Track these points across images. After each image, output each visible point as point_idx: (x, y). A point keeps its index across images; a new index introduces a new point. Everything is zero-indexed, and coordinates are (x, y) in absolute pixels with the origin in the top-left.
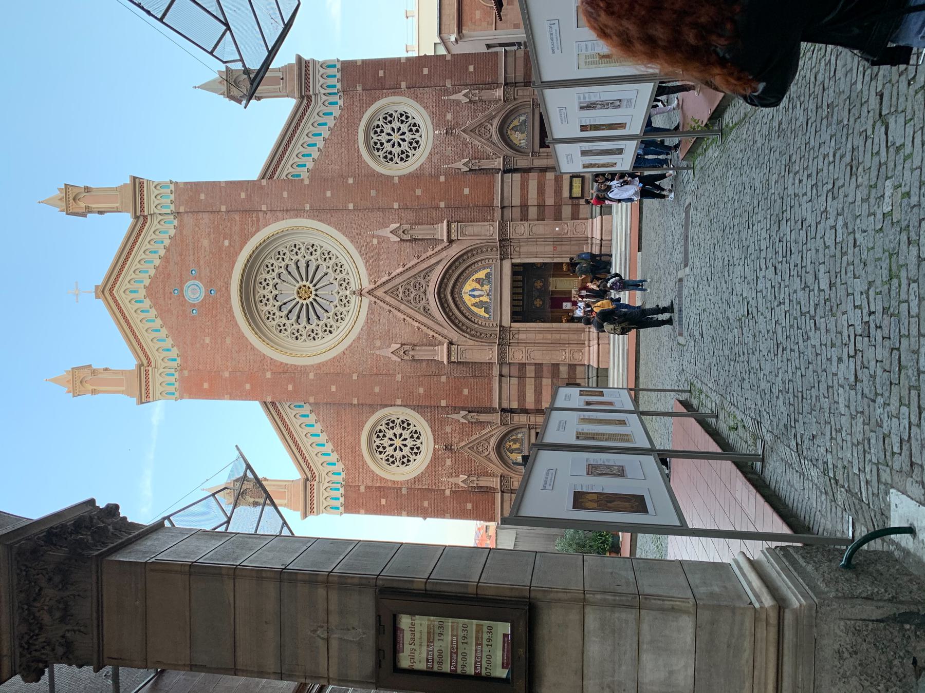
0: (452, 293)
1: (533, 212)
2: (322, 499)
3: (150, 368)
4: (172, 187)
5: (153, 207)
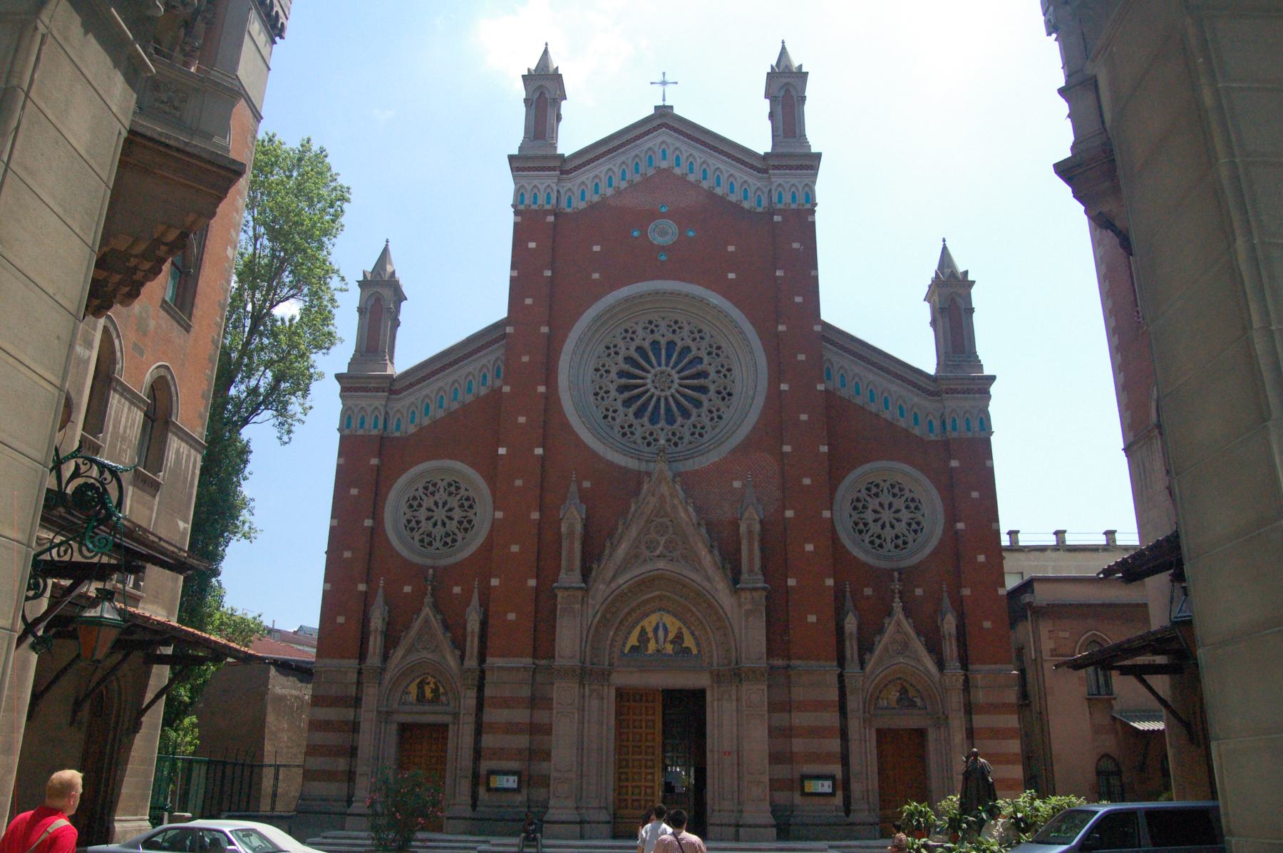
0: (660, 598)
1: (781, 719)
2: (363, 403)
4: (808, 206)
5: (781, 181)
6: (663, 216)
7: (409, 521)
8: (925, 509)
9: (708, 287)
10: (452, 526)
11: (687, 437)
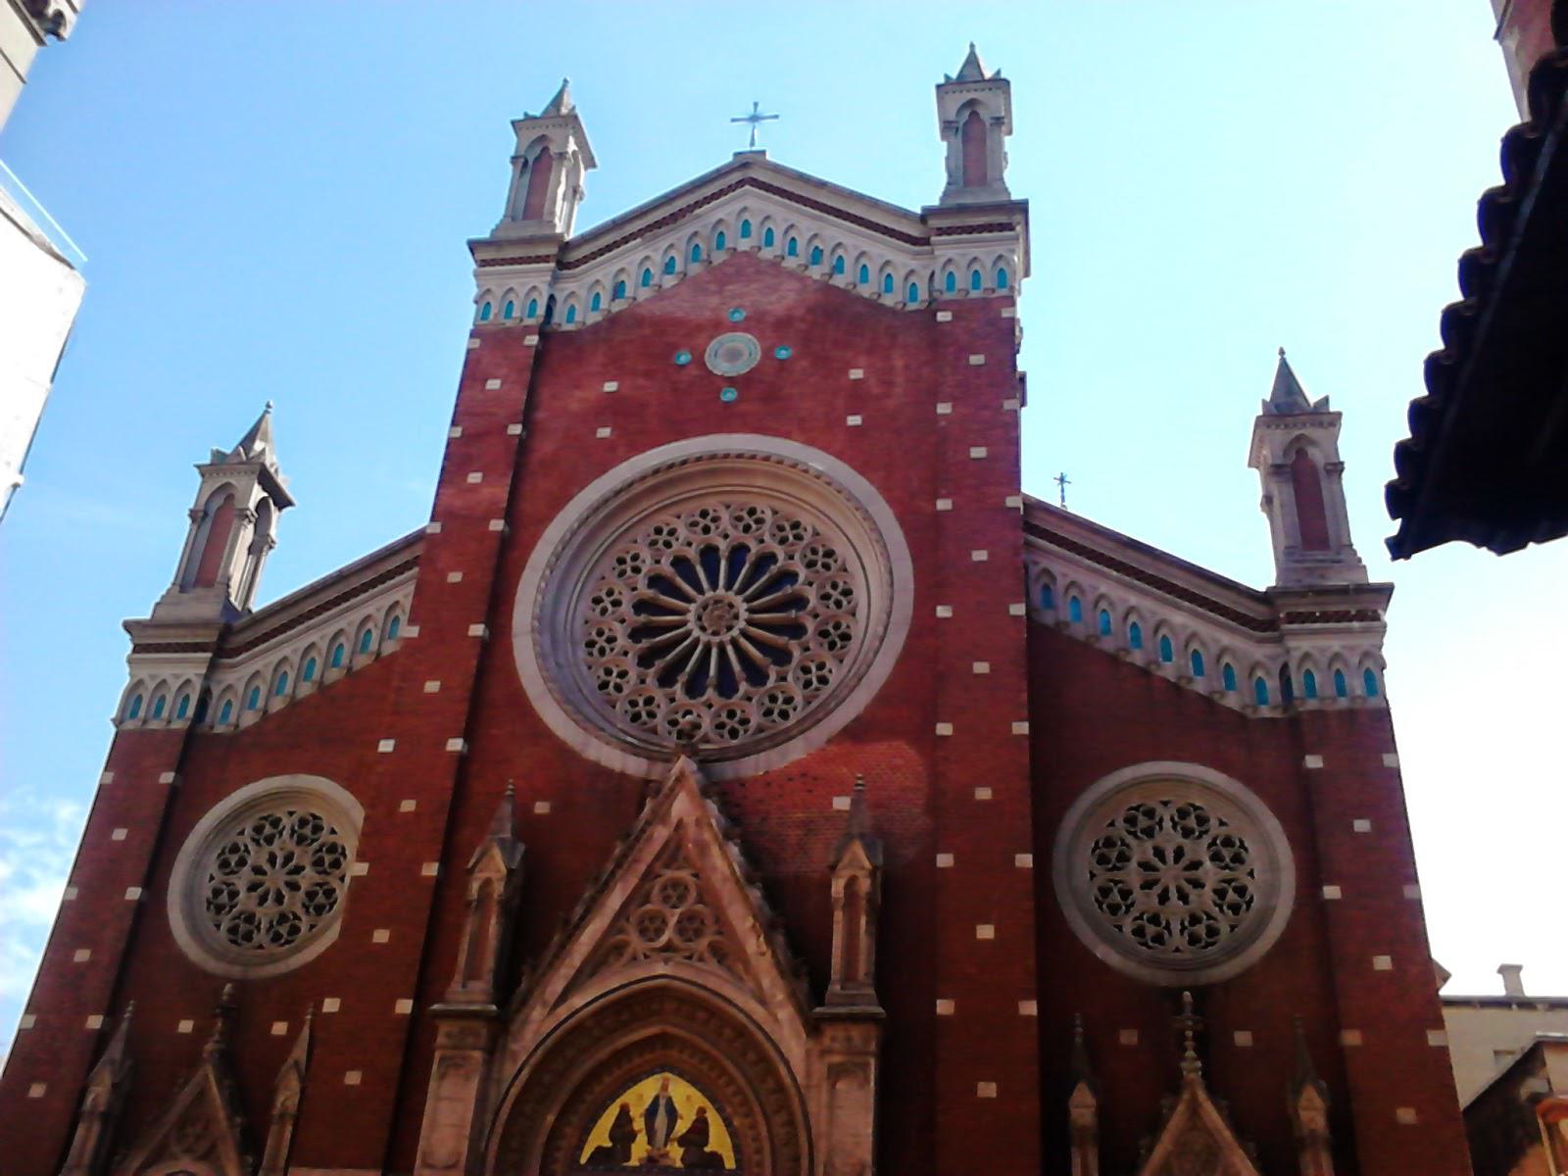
0: (663, 1039)
3: (552, 265)
4: (1004, 292)
6: (735, 327)
7: (217, 892)
8: (1254, 856)
9: (811, 442)
10: (294, 902)
11: (756, 719)
